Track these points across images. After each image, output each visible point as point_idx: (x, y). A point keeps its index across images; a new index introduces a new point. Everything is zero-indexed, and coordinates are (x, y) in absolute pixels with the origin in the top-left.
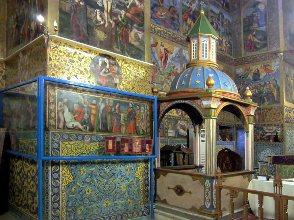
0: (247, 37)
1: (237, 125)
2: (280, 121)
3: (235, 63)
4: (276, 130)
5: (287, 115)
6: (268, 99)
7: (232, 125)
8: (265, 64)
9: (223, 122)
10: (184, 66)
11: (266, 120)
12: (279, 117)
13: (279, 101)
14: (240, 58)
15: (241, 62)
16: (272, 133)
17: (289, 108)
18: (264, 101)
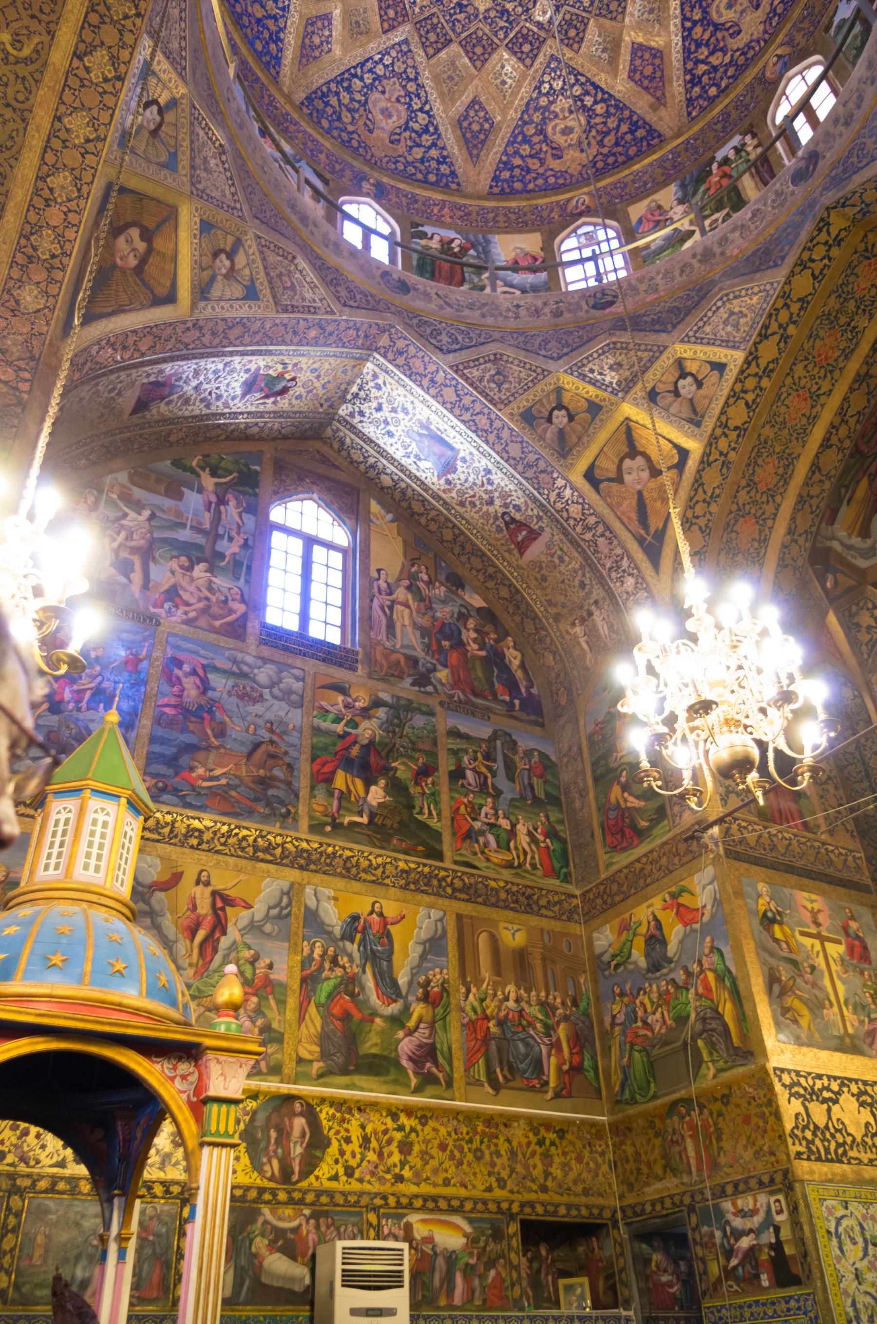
0: (607, 797)
1: (629, 1213)
2: (772, 1153)
3: (586, 909)
4: (769, 1212)
5: (805, 1122)
6: (712, 1046)
7: (607, 1214)
8: (673, 889)
9: (543, 1197)
10: (306, 951)
11: (722, 1160)
12: (765, 1131)
13: (748, 1050)
14: (597, 886)
15: (605, 902)
16: (757, 1232)
17: (820, 1077)
18: (699, 1062)
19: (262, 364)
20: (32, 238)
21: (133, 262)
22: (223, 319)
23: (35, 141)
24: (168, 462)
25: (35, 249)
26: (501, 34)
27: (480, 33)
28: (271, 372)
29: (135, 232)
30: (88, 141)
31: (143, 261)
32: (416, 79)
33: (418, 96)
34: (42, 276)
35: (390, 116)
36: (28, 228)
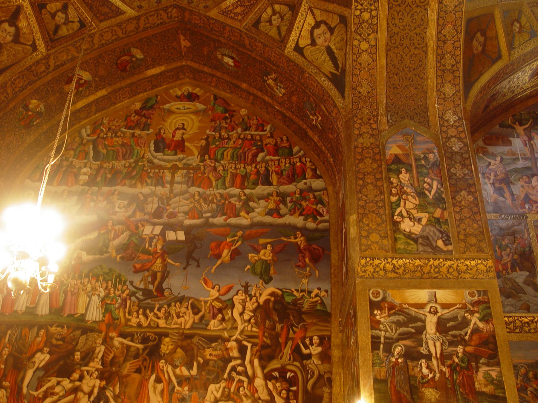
20: (442, 61)
21: (480, 48)
29: (479, 35)
30: (455, 6)
31: (484, 45)
34: (449, 77)
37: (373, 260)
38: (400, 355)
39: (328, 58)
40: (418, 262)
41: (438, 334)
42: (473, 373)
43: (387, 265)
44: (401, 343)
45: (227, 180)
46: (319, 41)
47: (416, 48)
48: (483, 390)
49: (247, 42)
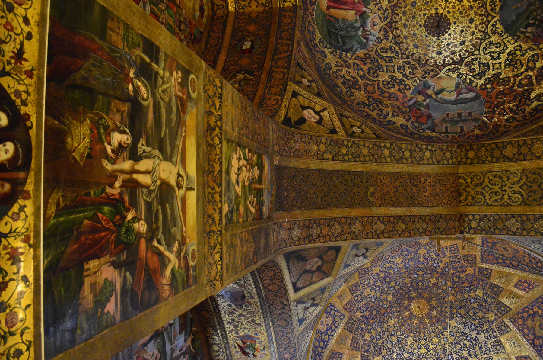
19: (262, 339)
21: (308, 268)
22: (290, 316)
23: (347, 212)
24: (191, 316)
25: (312, 227)
26: (363, 350)
27: (359, 342)
28: (257, 345)
29: (320, 263)
30: (354, 233)
32: (336, 327)
33: (332, 331)
35: (322, 325)
36: (317, 221)
37: (219, 98)
38: (136, 90)
39: (298, 118)
40: (217, 168)
41: (159, 182)
42: (112, 255)
43: (213, 119)
44: (150, 102)
45: (155, 8)
46: (305, 112)
47: (322, 198)
48: (86, 279)
49: (282, 56)
